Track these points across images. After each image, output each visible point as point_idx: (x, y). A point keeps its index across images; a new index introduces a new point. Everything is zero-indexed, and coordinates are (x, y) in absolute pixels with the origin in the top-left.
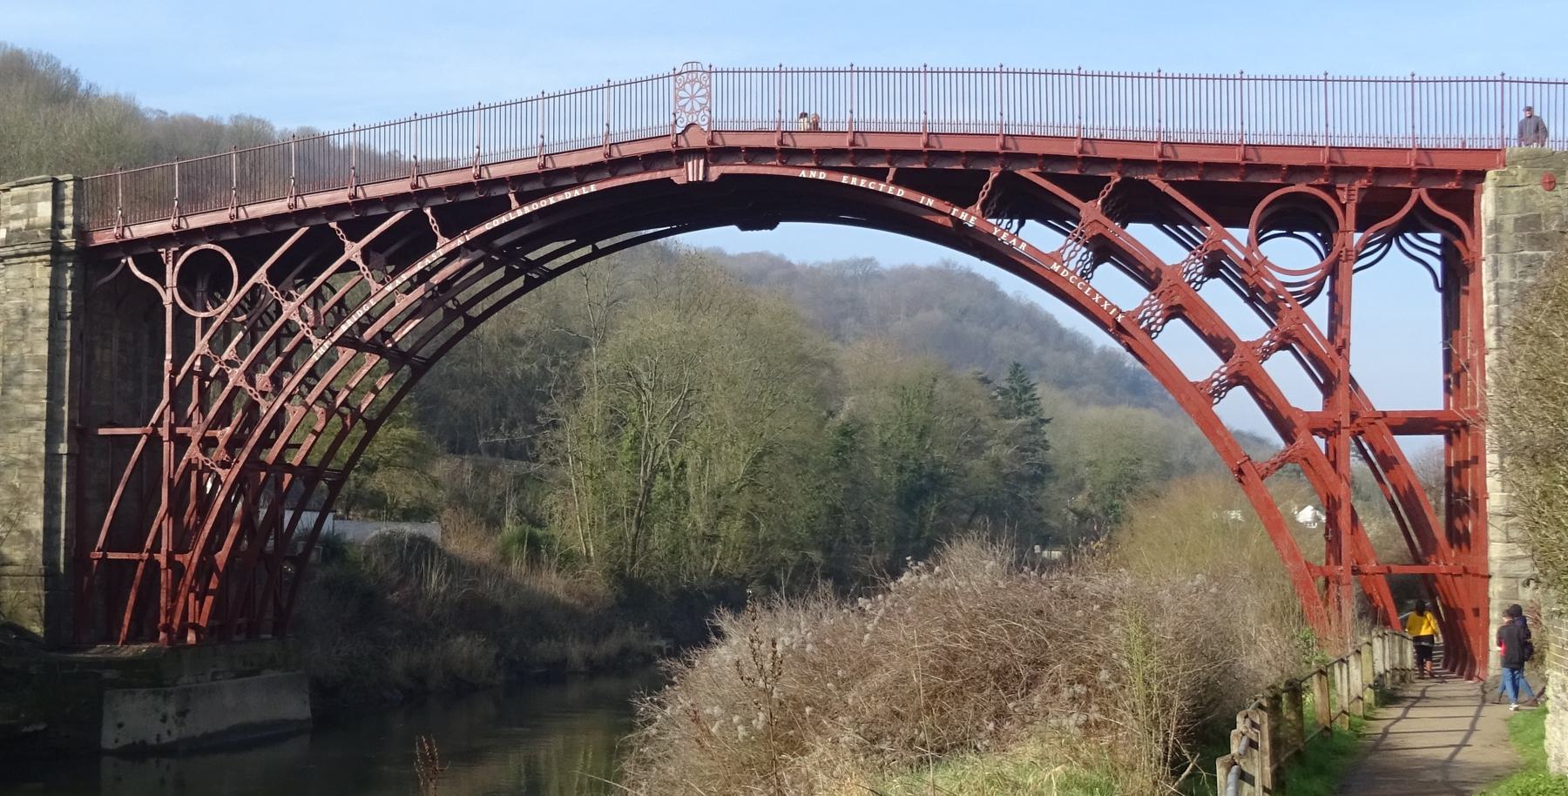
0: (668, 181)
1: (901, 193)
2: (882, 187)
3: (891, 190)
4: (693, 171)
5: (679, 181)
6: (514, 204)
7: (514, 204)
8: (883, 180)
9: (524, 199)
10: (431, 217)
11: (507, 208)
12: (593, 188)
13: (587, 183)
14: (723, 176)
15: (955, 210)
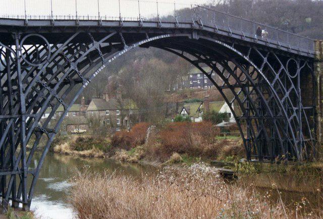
0: (187, 37)
1: (235, 50)
2: (232, 48)
3: (233, 49)
4: (196, 37)
5: (190, 38)
6: (148, 37)
7: (148, 37)
8: (231, 46)
9: (150, 36)
10: (122, 37)
11: (145, 38)
12: (169, 36)
13: (167, 34)
14: (200, 38)
15: (244, 57)
